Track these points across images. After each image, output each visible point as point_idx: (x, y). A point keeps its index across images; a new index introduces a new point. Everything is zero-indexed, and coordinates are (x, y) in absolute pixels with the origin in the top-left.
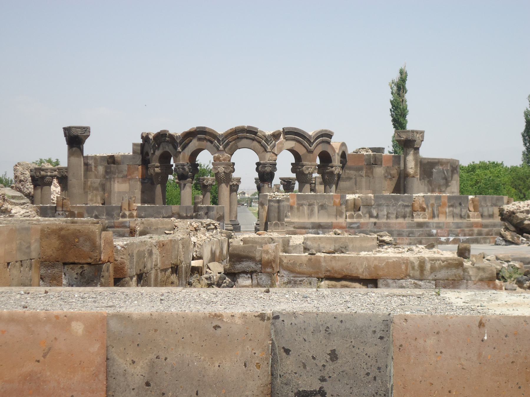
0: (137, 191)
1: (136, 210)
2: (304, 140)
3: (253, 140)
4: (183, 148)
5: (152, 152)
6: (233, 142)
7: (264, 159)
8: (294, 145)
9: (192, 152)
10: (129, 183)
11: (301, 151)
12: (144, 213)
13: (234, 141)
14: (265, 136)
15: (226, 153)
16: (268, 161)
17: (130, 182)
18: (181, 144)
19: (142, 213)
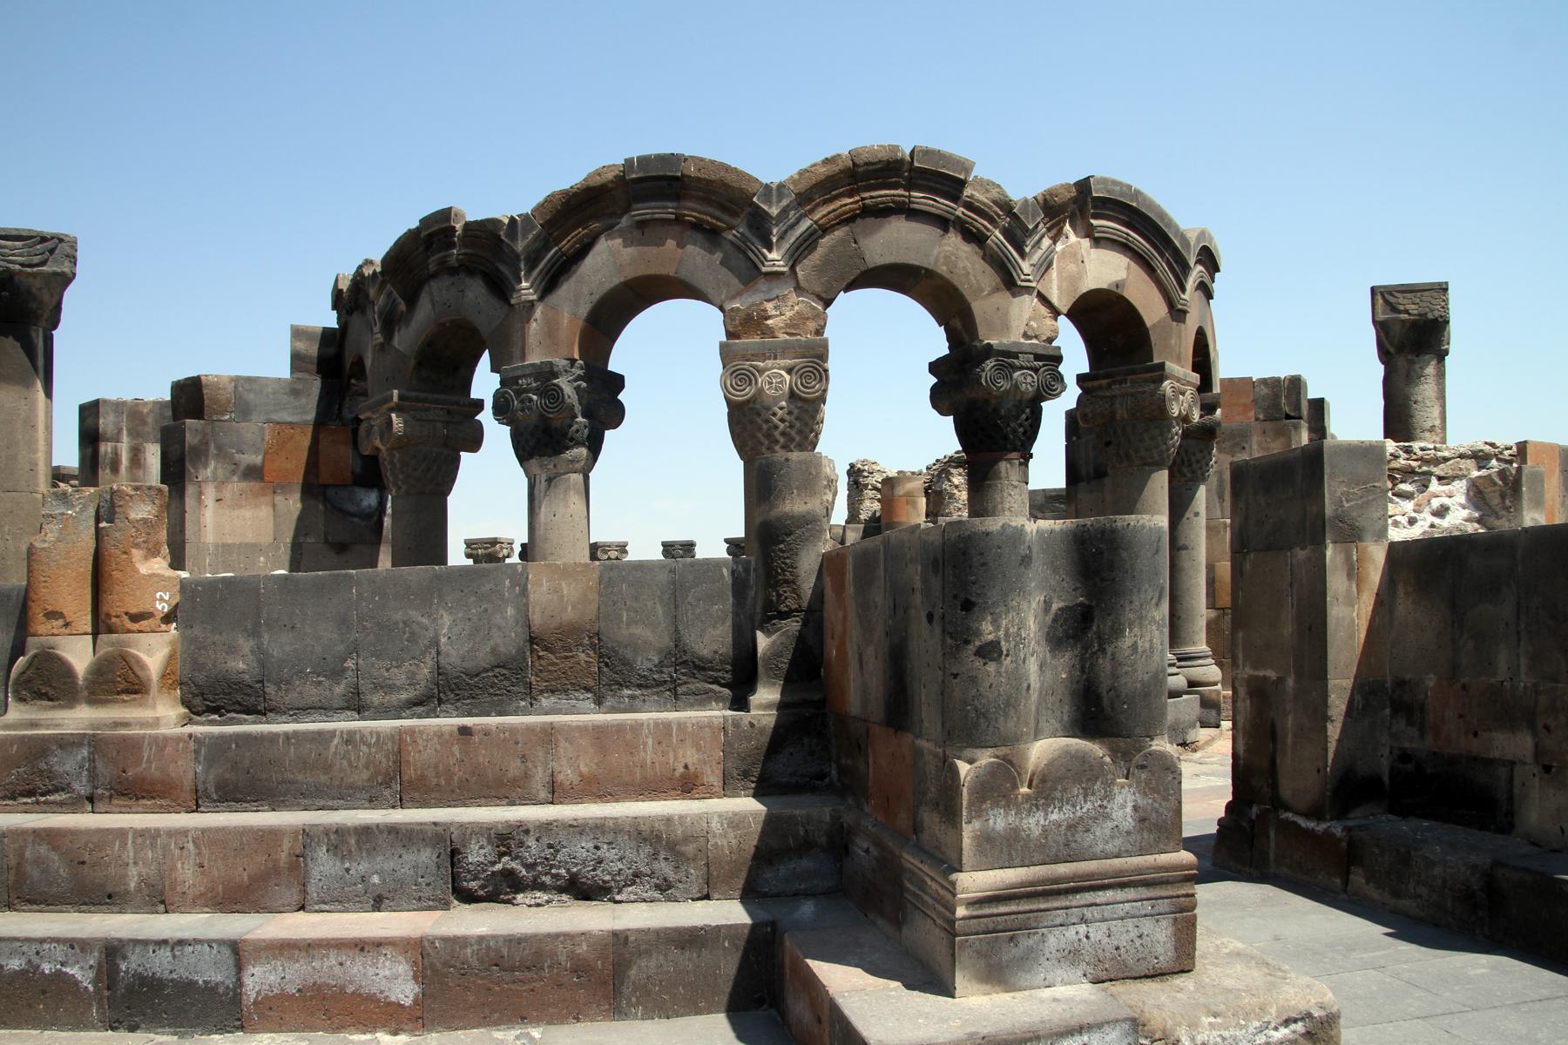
0: (309, 540)
1: (168, 618)
2: (1162, 255)
3: (943, 223)
4: (549, 285)
5: (379, 338)
6: (839, 233)
7: (1005, 327)
8: (1125, 276)
9: (596, 297)
10: (274, 506)
11: (1150, 305)
12: (246, 645)
13: (846, 229)
14: (1006, 206)
15: (799, 289)
16: (1022, 340)
17: (279, 499)
18: (533, 261)
19: (232, 650)
